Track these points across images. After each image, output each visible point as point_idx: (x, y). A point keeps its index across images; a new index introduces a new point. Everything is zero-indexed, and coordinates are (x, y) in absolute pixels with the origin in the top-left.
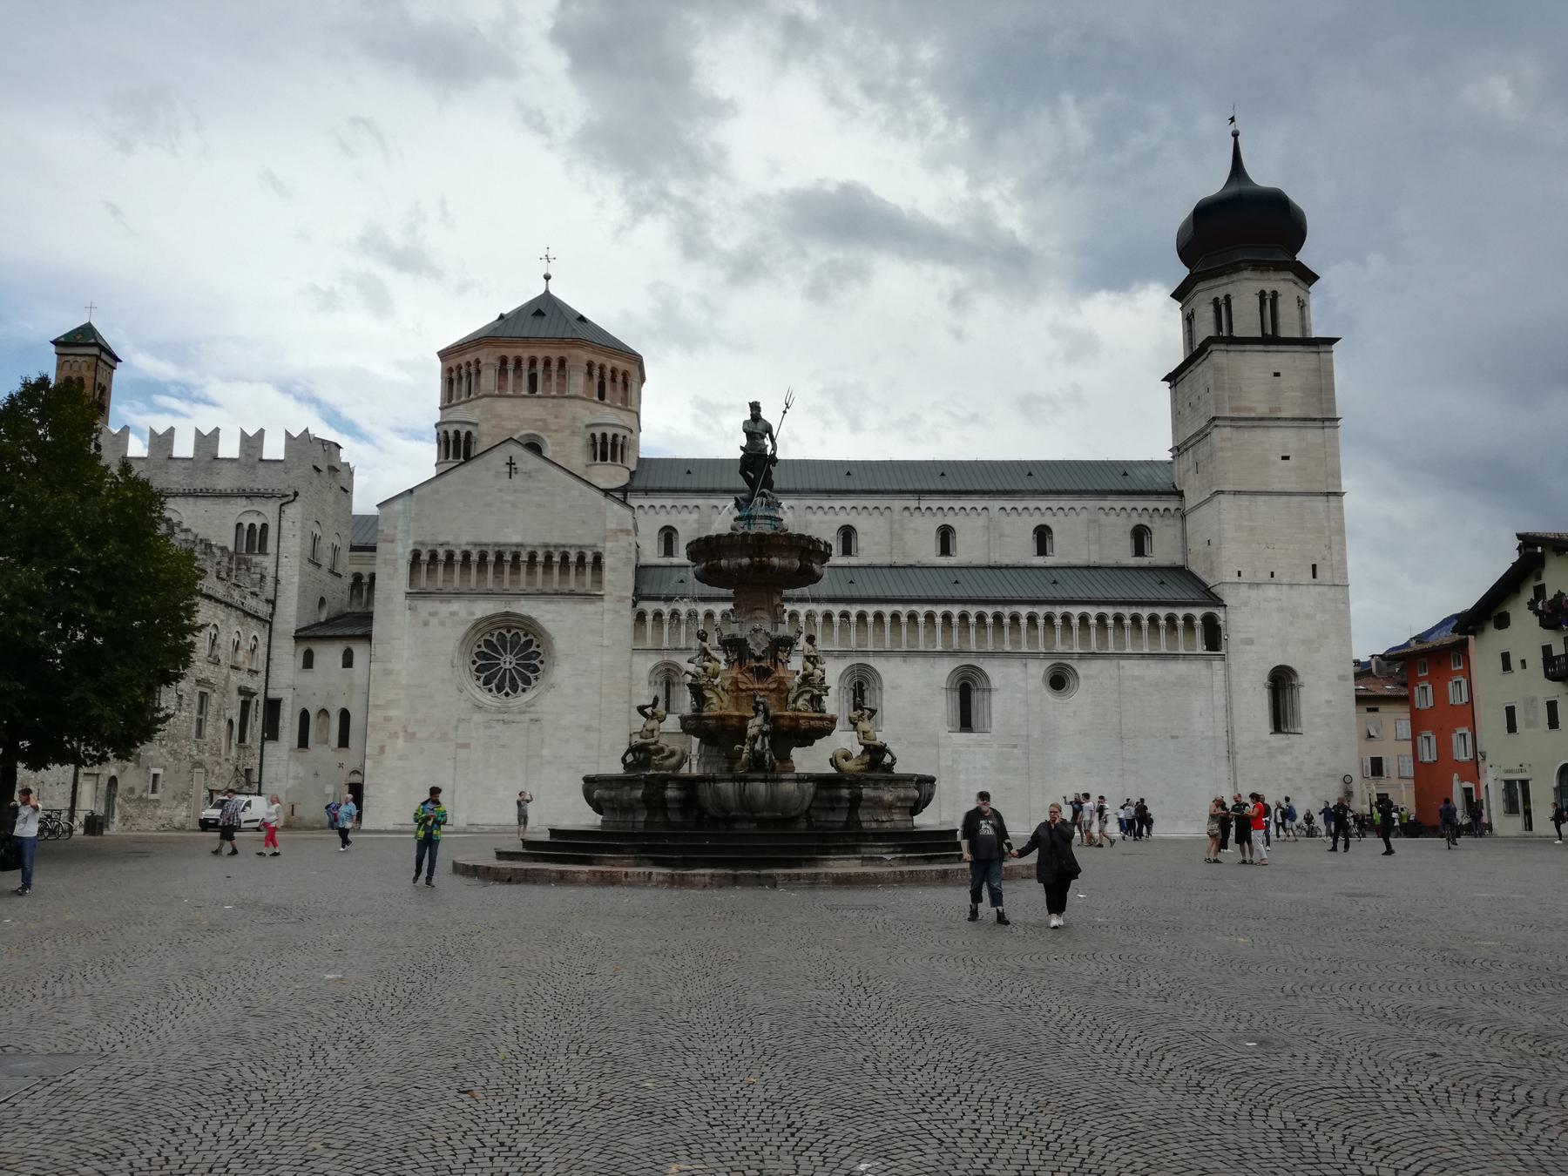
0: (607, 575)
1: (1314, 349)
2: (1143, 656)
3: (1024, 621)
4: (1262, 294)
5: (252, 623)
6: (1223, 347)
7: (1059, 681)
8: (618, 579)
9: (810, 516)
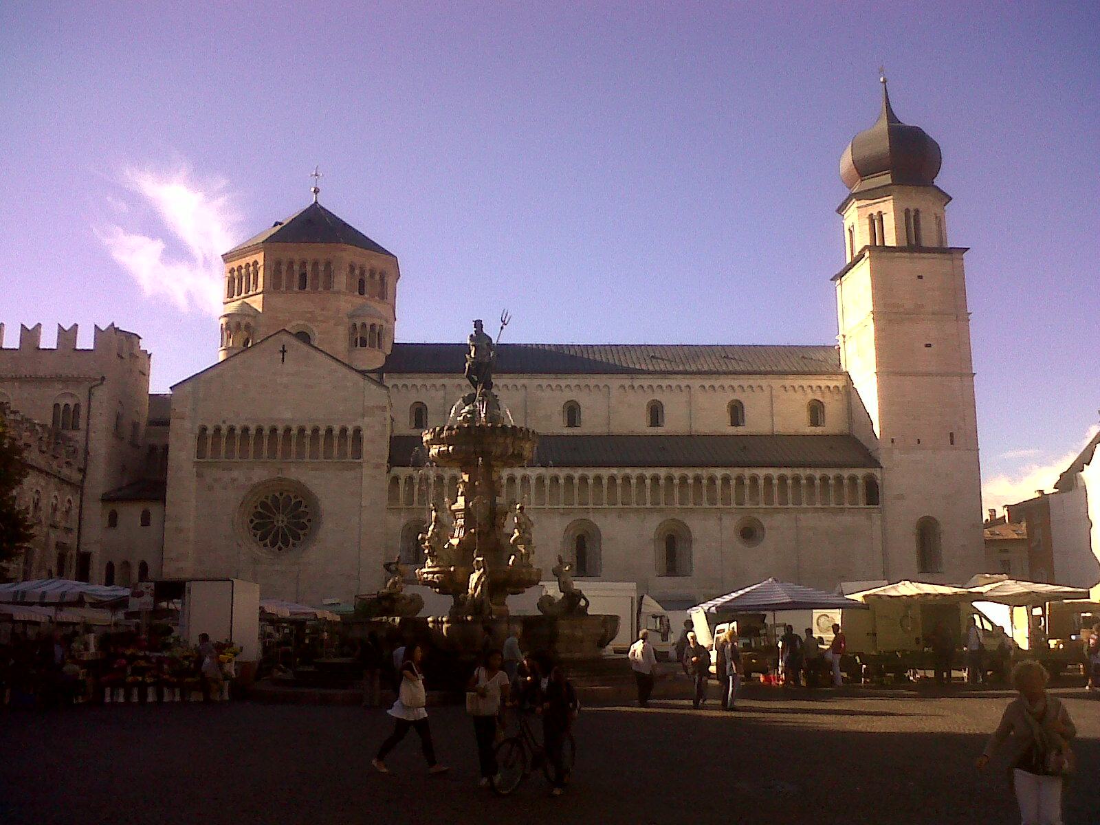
0: (366, 446)
2: (816, 510)
3: (719, 482)
4: (907, 211)
5: (67, 488)
7: (749, 533)
8: (376, 448)
9: (539, 393)
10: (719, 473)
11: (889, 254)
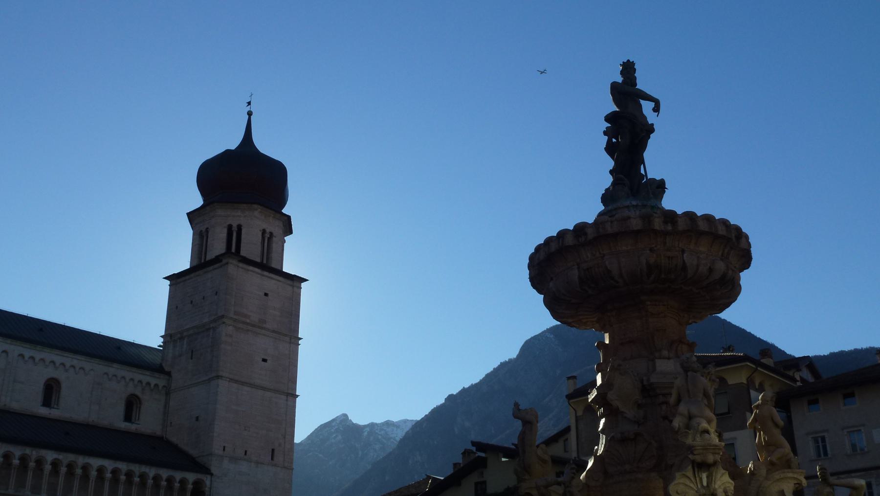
1: (289, 282)
3: (48, 468)
4: (264, 232)
6: (235, 262)
10: (50, 456)
11: (245, 266)
